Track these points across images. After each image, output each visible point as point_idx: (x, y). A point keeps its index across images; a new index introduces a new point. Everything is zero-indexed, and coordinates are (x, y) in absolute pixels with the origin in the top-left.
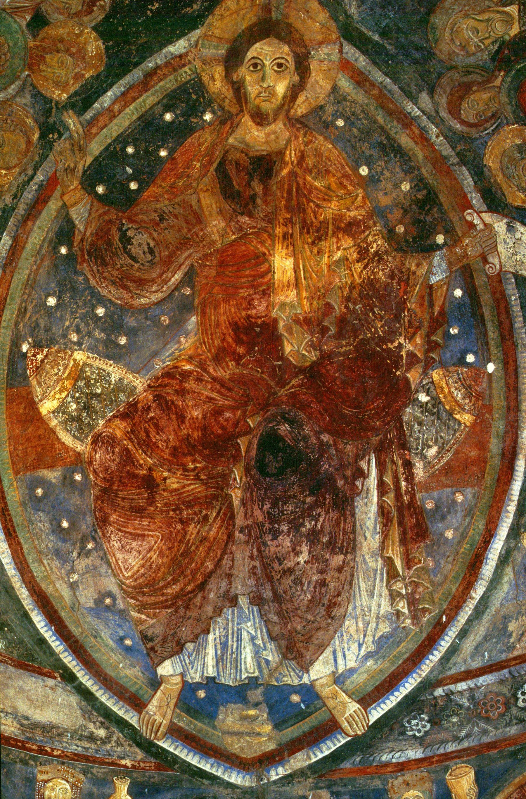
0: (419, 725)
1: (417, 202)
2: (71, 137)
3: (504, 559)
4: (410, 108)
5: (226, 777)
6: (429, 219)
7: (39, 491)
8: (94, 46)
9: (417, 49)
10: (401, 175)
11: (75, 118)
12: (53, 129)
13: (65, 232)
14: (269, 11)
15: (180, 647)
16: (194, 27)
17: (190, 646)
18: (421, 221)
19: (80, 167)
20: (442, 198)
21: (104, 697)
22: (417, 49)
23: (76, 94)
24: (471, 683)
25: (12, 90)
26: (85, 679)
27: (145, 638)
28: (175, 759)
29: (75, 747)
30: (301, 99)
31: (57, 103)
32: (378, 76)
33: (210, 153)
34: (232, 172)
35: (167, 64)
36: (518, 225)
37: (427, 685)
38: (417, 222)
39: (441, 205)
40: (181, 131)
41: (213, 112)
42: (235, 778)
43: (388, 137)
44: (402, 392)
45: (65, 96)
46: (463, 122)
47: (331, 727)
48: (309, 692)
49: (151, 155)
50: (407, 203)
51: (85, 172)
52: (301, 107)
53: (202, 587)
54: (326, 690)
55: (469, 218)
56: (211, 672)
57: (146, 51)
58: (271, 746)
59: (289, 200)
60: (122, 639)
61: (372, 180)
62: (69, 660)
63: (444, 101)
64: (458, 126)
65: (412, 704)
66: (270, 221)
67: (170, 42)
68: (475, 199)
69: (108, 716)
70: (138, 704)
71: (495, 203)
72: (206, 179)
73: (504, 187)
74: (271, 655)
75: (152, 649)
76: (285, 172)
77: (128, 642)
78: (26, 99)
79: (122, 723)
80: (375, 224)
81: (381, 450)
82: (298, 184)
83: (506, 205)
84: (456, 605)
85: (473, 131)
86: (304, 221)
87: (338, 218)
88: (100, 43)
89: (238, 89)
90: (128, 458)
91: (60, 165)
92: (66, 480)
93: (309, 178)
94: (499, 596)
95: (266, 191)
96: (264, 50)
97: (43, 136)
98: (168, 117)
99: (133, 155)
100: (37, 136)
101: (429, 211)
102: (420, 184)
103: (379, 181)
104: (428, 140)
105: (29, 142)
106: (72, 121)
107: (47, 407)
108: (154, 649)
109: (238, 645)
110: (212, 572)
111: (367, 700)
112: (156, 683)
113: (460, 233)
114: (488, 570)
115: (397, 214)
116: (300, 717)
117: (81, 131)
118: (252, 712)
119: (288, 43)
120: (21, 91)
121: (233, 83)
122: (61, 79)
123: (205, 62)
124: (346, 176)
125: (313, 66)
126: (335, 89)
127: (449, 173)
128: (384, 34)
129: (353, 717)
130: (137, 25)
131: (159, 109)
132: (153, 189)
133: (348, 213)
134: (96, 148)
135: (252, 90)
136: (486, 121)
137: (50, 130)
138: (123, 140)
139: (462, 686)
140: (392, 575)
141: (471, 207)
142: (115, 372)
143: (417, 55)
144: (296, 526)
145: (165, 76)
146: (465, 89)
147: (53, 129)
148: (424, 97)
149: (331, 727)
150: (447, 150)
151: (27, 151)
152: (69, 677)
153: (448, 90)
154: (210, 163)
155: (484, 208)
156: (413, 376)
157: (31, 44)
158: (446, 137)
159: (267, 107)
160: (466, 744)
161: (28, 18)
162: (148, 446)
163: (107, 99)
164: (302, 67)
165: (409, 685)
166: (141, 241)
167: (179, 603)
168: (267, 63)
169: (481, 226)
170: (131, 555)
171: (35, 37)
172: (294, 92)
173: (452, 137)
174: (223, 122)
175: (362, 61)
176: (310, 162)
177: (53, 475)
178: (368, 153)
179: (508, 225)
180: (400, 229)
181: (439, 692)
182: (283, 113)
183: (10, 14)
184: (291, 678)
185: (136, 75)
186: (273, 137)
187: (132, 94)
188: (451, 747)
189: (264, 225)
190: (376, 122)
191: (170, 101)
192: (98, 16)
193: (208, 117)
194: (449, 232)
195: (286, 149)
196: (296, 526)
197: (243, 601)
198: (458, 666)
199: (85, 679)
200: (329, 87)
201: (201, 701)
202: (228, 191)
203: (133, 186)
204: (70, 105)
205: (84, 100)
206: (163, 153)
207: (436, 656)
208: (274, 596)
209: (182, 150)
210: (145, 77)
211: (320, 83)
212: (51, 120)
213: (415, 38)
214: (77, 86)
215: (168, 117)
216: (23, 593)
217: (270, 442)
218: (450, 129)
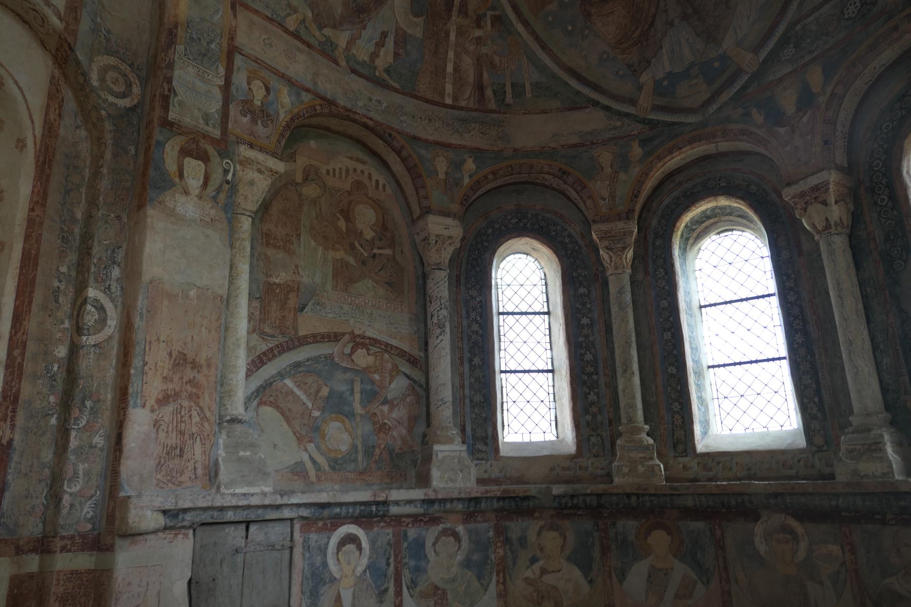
5: (686, 121)
7: (550, 19)
15: (649, 62)
17: (653, 60)
24: (816, 14)
27: (629, 66)
28: (658, 122)
42: (692, 119)
47: (739, 72)
53: (652, 24)
56: (668, 69)
58: (707, 96)
60: (617, 73)
65: (784, 41)
69: (619, 114)
70: (633, 102)
75: (635, 70)
77: (621, 73)
79: (627, 115)
110: (655, 15)
111: (756, 50)
112: (640, 88)
118: (694, 82)
139: (811, 18)
152: (596, 104)
160: (815, 53)
181: (798, 27)
188: (808, 58)
197: (676, 22)
199: (604, 101)
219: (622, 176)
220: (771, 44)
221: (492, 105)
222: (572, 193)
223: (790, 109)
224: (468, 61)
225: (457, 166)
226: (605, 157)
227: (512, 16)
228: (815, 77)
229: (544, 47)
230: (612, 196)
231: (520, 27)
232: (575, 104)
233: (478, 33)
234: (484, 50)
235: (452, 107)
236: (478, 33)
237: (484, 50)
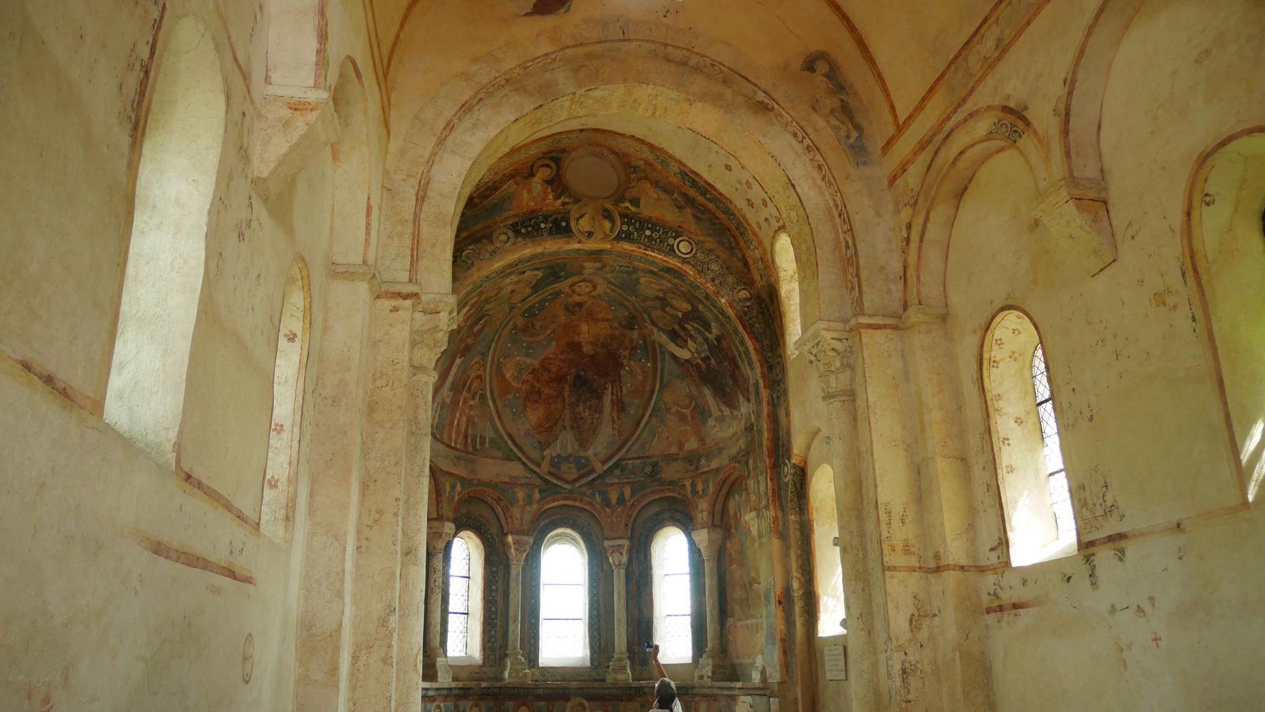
0: (617, 472)
3: (647, 424)
13: (515, 327)
21: (529, 464)
26: (524, 460)
29: (523, 481)
37: (621, 460)
42: (566, 486)
44: (621, 366)
47: (593, 471)
48: (587, 459)
54: (592, 458)
62: (519, 454)
65: (616, 465)
69: (531, 470)
70: (539, 465)
71: (653, 323)
74: (576, 446)
81: (612, 382)
84: (632, 435)
90: (533, 386)
92: (515, 398)
94: (644, 435)
107: (508, 375)
108: (543, 446)
109: (566, 443)
111: (604, 463)
112: (543, 458)
114: (642, 425)
116: (584, 467)
129: (600, 468)
140: (614, 422)
142: (529, 361)
144: (584, 403)
149: (593, 471)
152: (519, 459)
156: (625, 362)
162: (538, 381)
165: (616, 459)
166: (537, 325)
167: (548, 429)
170: (534, 415)
177: (510, 396)
184: (582, 454)
196: (584, 403)
198: (629, 456)
199: (524, 460)
201: (556, 463)
207: (624, 451)
208: (577, 426)
216: (505, 435)
217: (578, 377)
219: (528, 508)
220: (610, 463)
221: (470, 449)
222: (499, 510)
223: (614, 501)
224: (464, 419)
225: (453, 487)
226: (521, 495)
227: (489, 395)
228: (627, 491)
229: (500, 418)
230: (522, 518)
231: (490, 403)
232: (510, 457)
233: (472, 403)
234: (472, 413)
235: (454, 449)
236: (472, 403)
237: (472, 413)
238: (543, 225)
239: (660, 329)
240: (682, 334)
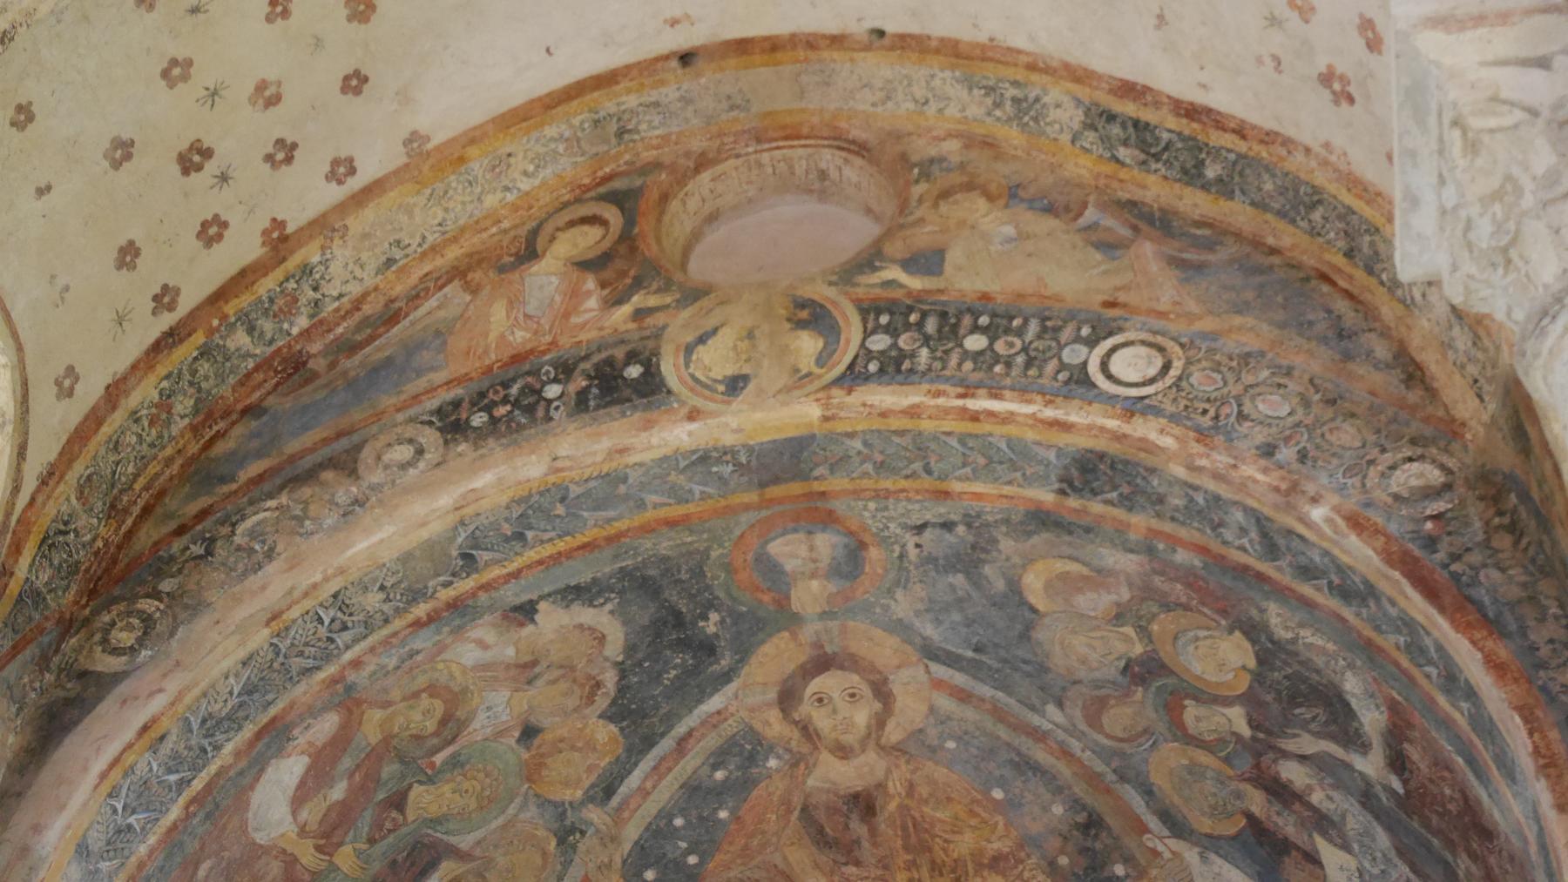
1: (1077, 826)
2: (598, 831)
4: (1036, 720)
6: (1098, 846)
8: (605, 733)
9: (1025, 662)
10: (1048, 796)
11: (599, 811)
12: (572, 830)
14: (822, 647)
16: (729, 681)
18: (1088, 849)
19: (618, 860)
20: (1110, 820)
22: (1025, 662)
23: (593, 786)
25: (511, 811)
30: (891, 725)
31: (571, 803)
32: (986, 691)
33: (786, 804)
34: (821, 816)
35: (703, 723)
36: (1213, 856)
38: (1084, 851)
39: (1109, 829)
40: (742, 786)
41: (779, 757)
43: (1019, 754)
45: (579, 793)
46: (1108, 736)
49: (707, 822)
50: (1064, 828)
51: (624, 862)
52: (893, 734)
55: (1150, 845)
57: (670, 720)
59: (906, 837)
61: (1011, 805)
63: (1078, 713)
64: (1105, 741)
66: (886, 867)
67: (700, 701)
68: (1153, 823)
71: (1177, 827)
72: (788, 831)
73: (1185, 811)
76: (892, 806)
78: (532, 811)
80: (1029, 856)
82: (913, 818)
83: (1192, 831)
85: (1125, 745)
86: (933, 862)
87: (977, 855)
88: (612, 727)
89: (807, 731)
91: (591, 865)
93: (926, 810)
95: (873, 832)
96: (829, 683)
97: (561, 842)
98: (719, 775)
99: (684, 828)
100: (554, 843)
101: (1096, 836)
102: (1076, 804)
103: (1021, 805)
104: (1072, 755)
105: (544, 854)
106: (594, 814)
113: (1143, 862)
115: (1055, 843)
117: (608, 820)
119: (857, 672)
120: (523, 806)
121: (796, 723)
122: (569, 778)
123: (752, 710)
124: (974, 801)
125: (896, 689)
126: (932, 710)
127: (1108, 791)
128: (976, 650)
130: (653, 697)
131: (706, 770)
132: (720, 857)
133: (990, 846)
134: (632, 832)
135: (822, 721)
136: (1140, 735)
137: (567, 834)
138: (666, 815)
141: (1148, 831)
143: (1028, 668)
145: (703, 736)
146: (1101, 704)
147: (572, 830)
148: (1051, 709)
150: (1099, 767)
151: (544, 867)
153: (1080, 703)
154: (789, 811)
155: (1166, 832)
157: (526, 755)
158: (1094, 752)
159: (849, 739)
161: (517, 734)
163: (634, 780)
164: (882, 692)
168: (835, 695)
169: (1167, 855)
171: (528, 749)
172: (880, 722)
173: (1099, 752)
174: (795, 765)
175: (960, 679)
176: (924, 791)
178: (997, 773)
179: (1201, 855)
180: (1063, 861)
182: (872, 743)
183: (495, 740)
185: (666, 745)
186: (866, 769)
187: (665, 765)
189: (879, 872)
190: (998, 738)
191: (718, 759)
192: (602, 703)
193: (772, 763)
194: (1128, 860)
195: (887, 778)
200: (924, 708)
202: (822, 839)
203: (692, 860)
204: (589, 798)
205: (606, 789)
206: (723, 814)
209: (746, 806)
210: (679, 744)
211: (911, 708)
212: (568, 822)
213: (1020, 653)
214: (593, 778)
215: (719, 775)
218: (1096, 743)
238: (552, 391)
239: (1210, 843)
240: (1287, 825)
